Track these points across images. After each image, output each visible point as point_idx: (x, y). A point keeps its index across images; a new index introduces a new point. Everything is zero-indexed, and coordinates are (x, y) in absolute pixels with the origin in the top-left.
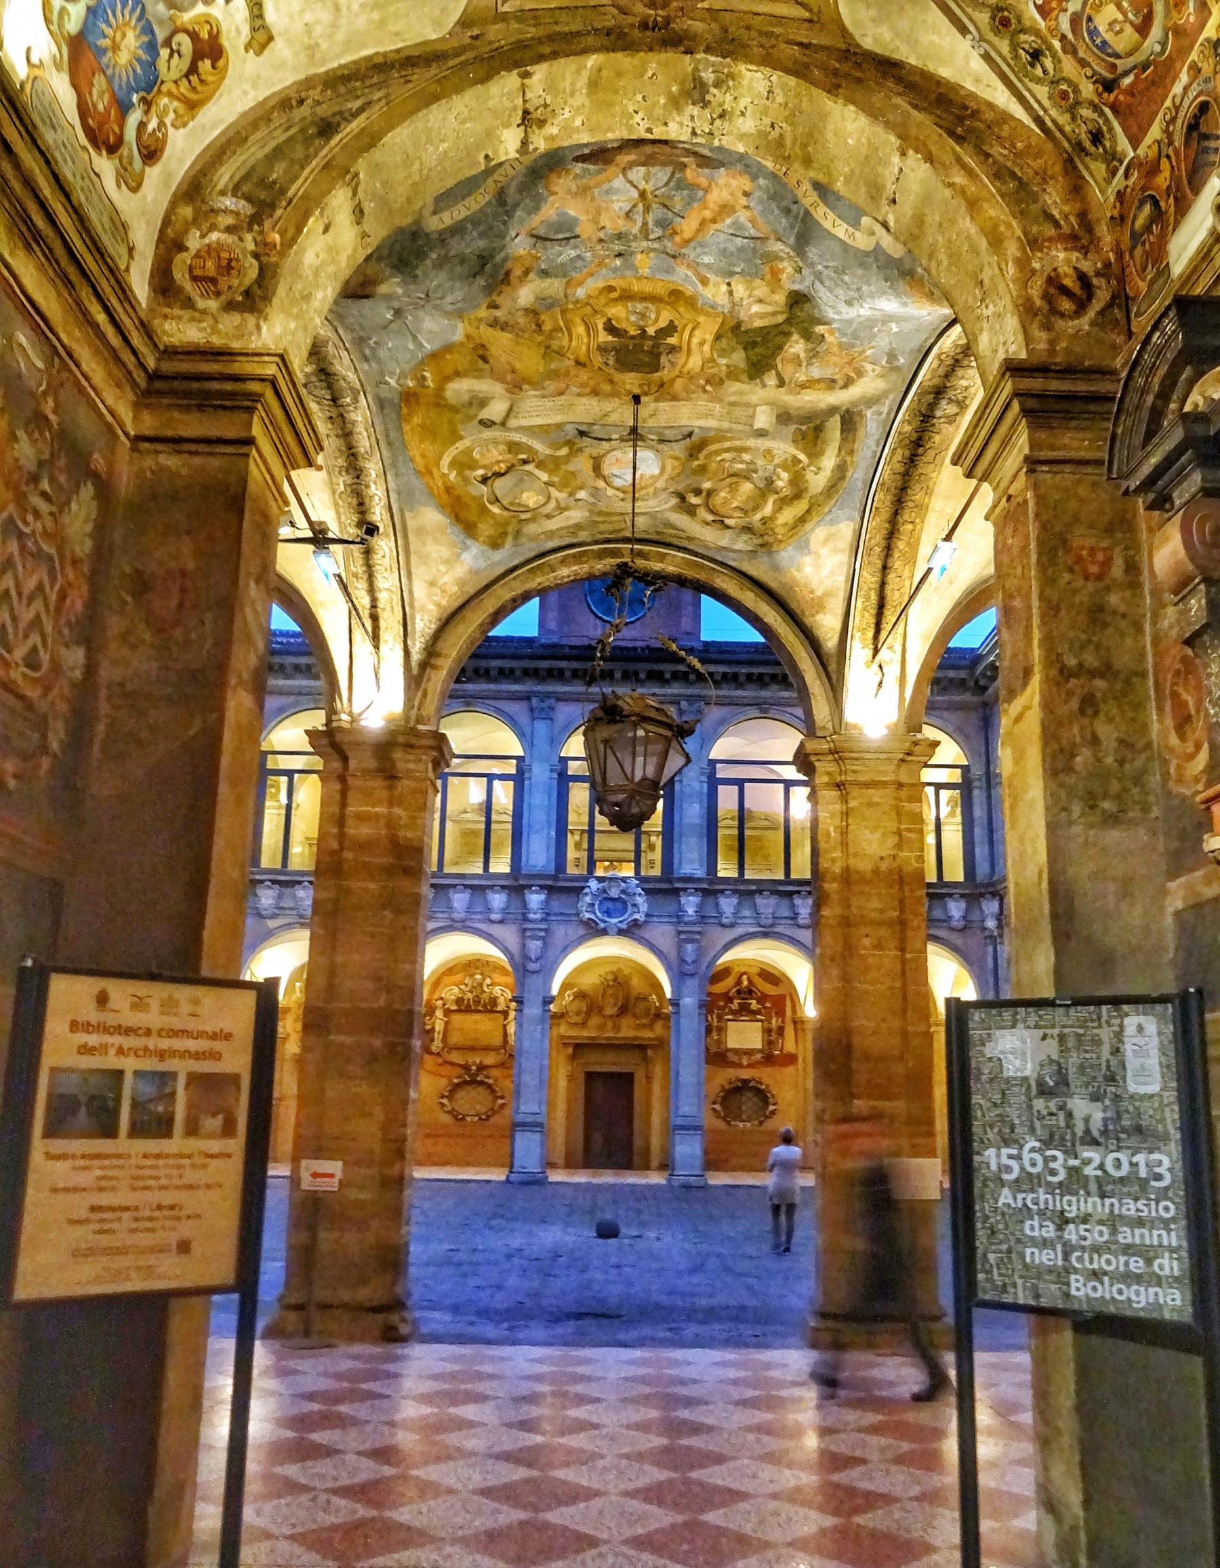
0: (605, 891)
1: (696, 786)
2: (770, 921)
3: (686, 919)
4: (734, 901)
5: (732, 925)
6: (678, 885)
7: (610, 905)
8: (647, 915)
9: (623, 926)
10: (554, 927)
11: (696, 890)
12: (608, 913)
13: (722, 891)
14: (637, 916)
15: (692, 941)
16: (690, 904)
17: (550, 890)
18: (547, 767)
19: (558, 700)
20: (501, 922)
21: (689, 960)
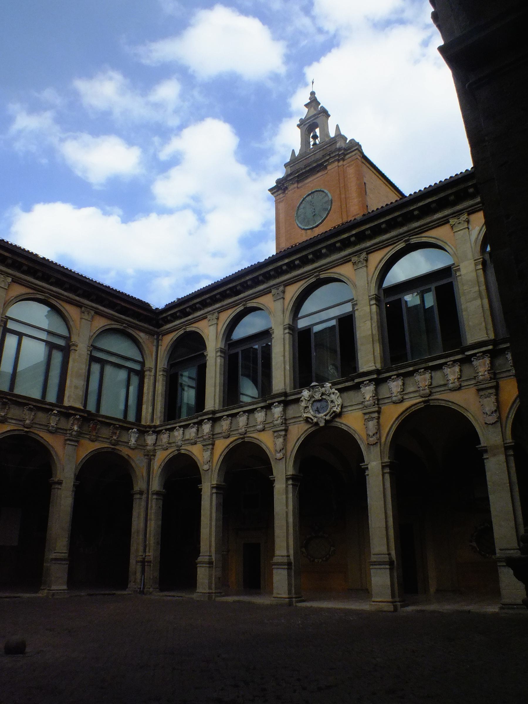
0: (313, 397)
1: (367, 309)
2: (428, 391)
3: (366, 403)
4: (400, 382)
5: (402, 401)
6: (357, 381)
7: (318, 405)
8: (342, 408)
9: (328, 418)
10: (291, 428)
11: (370, 381)
12: (318, 411)
13: (390, 377)
14: (335, 409)
15: (372, 419)
16: (368, 391)
17: (286, 404)
18: (281, 328)
19: (286, 286)
20: (263, 430)
21: (371, 434)
